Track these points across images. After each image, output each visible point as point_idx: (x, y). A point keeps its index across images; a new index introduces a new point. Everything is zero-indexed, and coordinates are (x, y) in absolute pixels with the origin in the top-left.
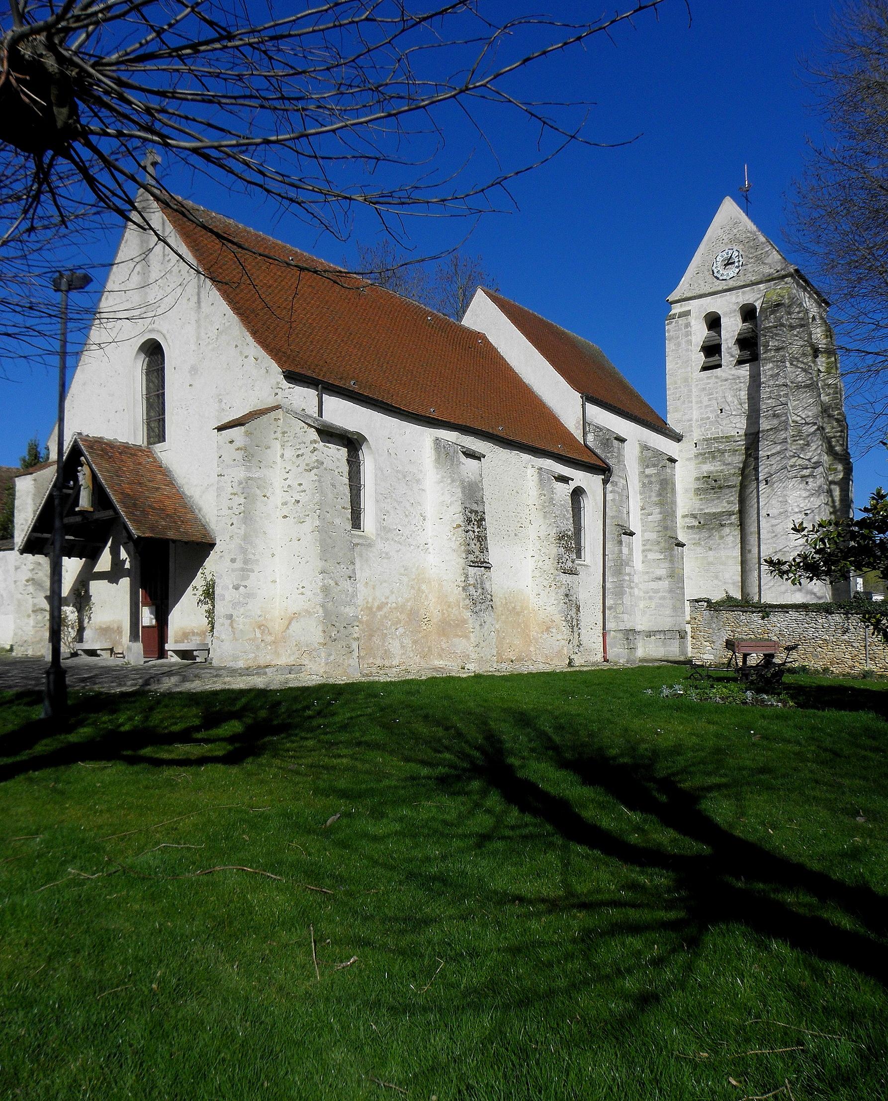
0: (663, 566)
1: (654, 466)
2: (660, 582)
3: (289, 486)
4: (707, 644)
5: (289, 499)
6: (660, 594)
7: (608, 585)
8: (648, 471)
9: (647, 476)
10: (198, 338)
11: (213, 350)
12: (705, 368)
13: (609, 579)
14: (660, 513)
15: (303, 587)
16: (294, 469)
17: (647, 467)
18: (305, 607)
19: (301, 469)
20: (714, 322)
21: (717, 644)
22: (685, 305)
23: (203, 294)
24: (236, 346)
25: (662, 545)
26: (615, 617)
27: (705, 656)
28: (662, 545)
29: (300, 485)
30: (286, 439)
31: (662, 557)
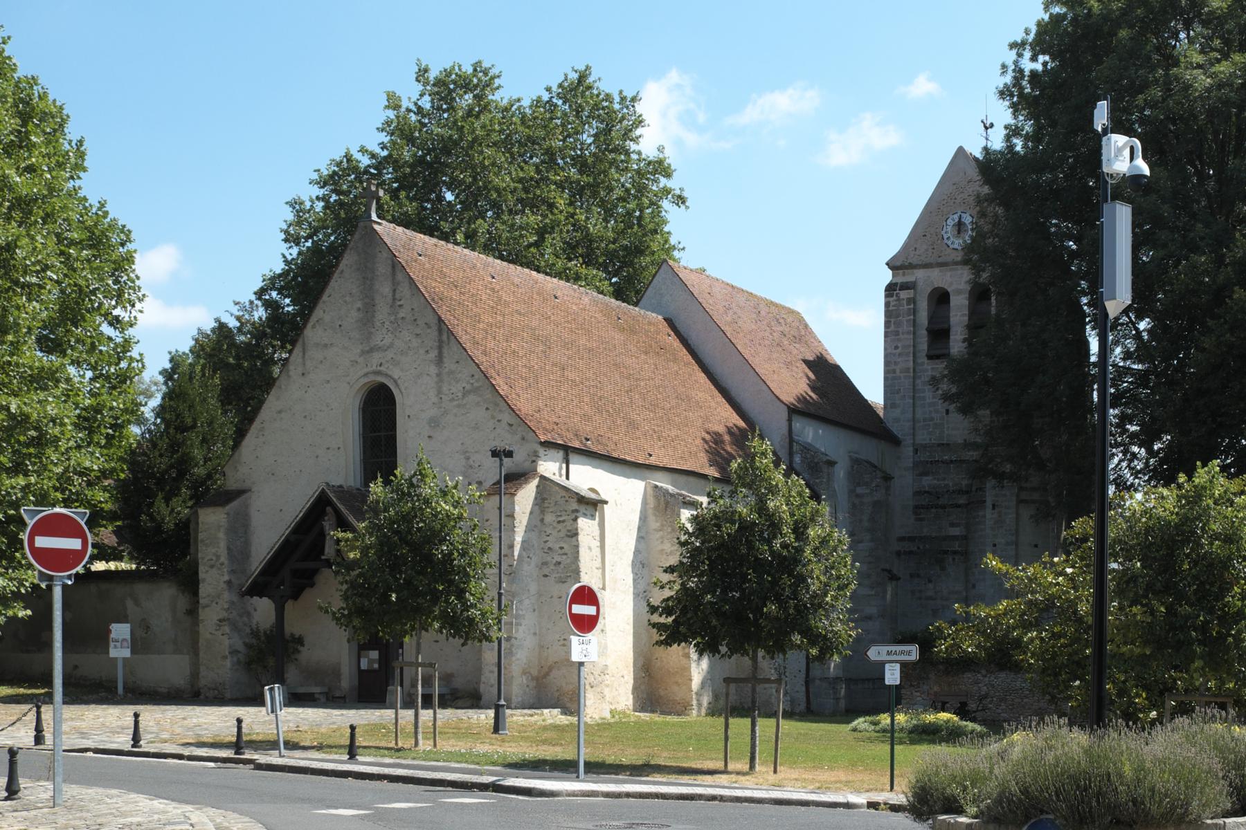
5: (549, 559)
8: (859, 490)
9: (858, 496)
10: (439, 392)
11: (458, 406)
16: (554, 533)
17: (858, 484)
19: (562, 534)
23: (445, 351)
29: (562, 548)
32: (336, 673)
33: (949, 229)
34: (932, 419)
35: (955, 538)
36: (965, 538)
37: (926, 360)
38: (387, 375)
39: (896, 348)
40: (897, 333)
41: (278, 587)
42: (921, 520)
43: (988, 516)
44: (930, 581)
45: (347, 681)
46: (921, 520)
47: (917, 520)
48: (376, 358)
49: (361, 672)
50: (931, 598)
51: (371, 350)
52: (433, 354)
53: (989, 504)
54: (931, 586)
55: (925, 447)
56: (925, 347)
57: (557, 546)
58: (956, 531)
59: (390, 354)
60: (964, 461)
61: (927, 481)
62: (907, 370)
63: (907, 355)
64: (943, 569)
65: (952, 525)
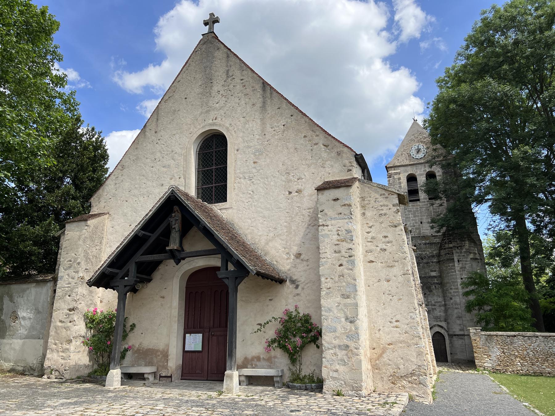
3: (373, 238)
4: (486, 356)
15: (397, 321)
18: (401, 338)
20: (412, 179)
22: (396, 170)
24: (305, 137)
27: (485, 364)
29: (385, 237)
30: (366, 202)
32: (165, 355)
33: (413, 152)
38: (220, 125)
41: (123, 278)
43: (456, 265)
45: (174, 361)
48: (212, 114)
49: (185, 352)
51: (208, 112)
52: (259, 105)
53: (456, 260)
57: (380, 236)
58: (433, 274)
59: (222, 112)
64: (431, 291)
65: (432, 271)
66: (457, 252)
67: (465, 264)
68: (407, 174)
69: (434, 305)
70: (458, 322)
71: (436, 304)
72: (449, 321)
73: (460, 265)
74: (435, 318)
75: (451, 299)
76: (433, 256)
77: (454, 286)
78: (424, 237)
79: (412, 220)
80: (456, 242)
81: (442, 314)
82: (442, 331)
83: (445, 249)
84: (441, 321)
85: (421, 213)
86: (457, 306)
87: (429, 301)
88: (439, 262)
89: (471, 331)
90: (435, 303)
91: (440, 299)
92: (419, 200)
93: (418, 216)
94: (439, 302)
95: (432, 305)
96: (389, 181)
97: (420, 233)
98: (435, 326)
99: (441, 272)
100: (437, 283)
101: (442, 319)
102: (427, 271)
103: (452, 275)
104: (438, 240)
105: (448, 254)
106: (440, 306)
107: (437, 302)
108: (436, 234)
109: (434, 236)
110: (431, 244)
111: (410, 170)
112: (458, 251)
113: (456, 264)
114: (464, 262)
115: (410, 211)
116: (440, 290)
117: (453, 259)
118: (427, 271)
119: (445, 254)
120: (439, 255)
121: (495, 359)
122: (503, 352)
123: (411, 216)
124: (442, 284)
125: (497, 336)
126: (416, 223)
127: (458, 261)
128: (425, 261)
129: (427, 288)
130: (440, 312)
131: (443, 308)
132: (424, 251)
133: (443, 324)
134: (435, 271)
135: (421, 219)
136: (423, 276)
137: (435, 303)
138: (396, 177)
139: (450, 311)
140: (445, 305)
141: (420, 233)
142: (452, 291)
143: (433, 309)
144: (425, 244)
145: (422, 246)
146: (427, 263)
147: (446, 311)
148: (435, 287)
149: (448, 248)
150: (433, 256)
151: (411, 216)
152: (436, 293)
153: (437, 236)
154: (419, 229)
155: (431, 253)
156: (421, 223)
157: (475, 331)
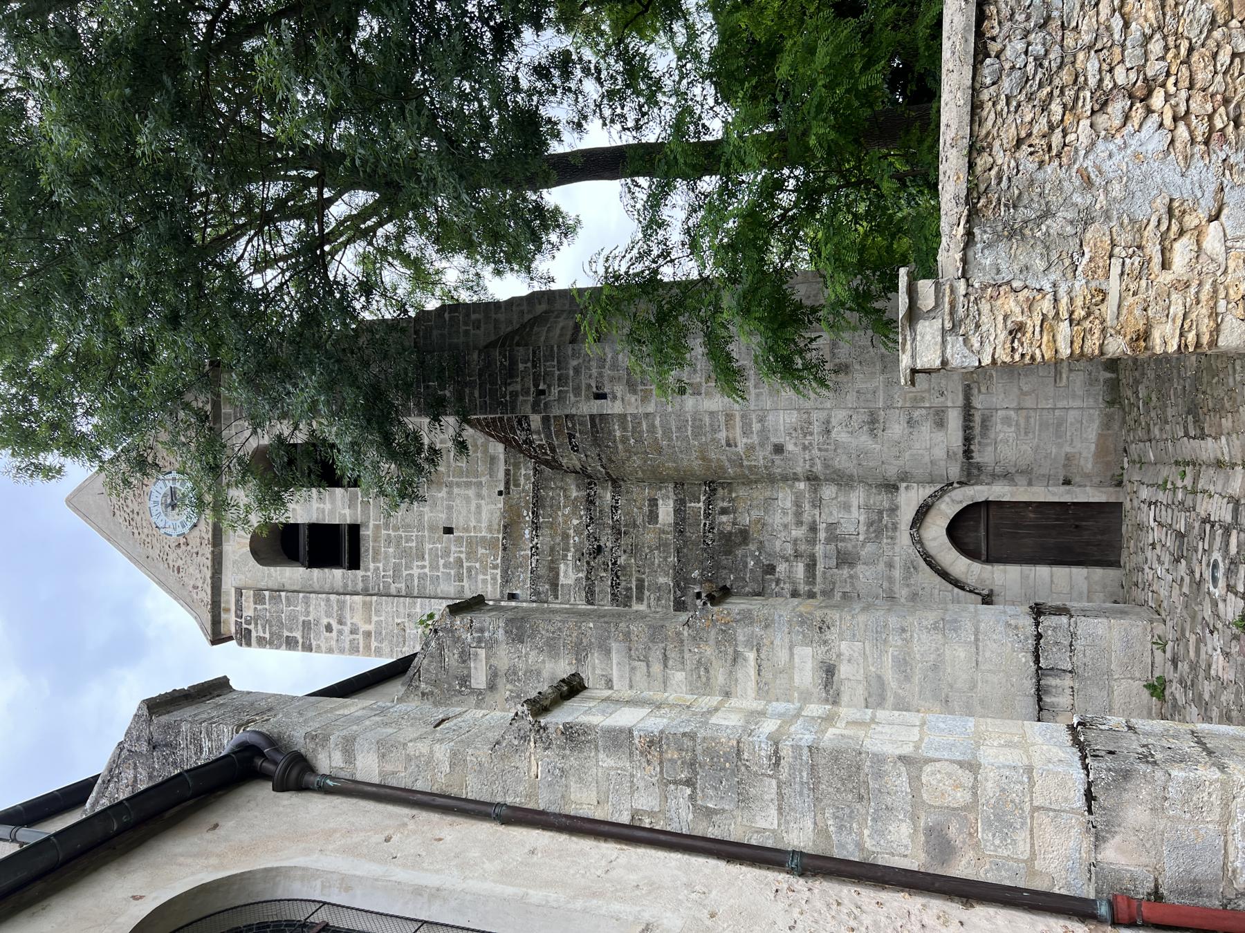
0: (782, 655)
1: (465, 657)
2: (844, 670)
4: (1181, 252)
6: (890, 676)
7: (800, 837)
8: (479, 679)
9: (492, 687)
12: (355, 564)
13: (761, 824)
14: (608, 652)
17: (465, 680)
21: (1182, 188)
22: (228, 602)
25: (709, 651)
26: (1002, 823)
28: (709, 651)
31: (751, 656)
34: (459, 562)
35: (679, 511)
36: (679, 484)
37: (360, 573)
39: (329, 628)
40: (306, 625)
42: (640, 588)
44: (771, 569)
46: (640, 588)
47: (640, 599)
50: (811, 567)
53: (595, 407)
54: (782, 568)
55: (506, 581)
56: (338, 573)
58: (666, 512)
60: (536, 496)
61: (569, 575)
62: (367, 606)
63: (341, 606)
64: (744, 535)
65: (653, 517)
66: (562, 398)
67: (614, 366)
68: (252, 561)
69: (813, 529)
70: (897, 429)
71: (806, 518)
72: (892, 472)
73: (619, 389)
74: (879, 533)
75: (779, 449)
76: (590, 501)
77: (715, 430)
78: (510, 528)
79: (434, 567)
80: (514, 395)
81: (857, 497)
82: (947, 509)
83: (553, 450)
84: (894, 510)
85: (407, 527)
86: (816, 428)
87: (789, 550)
88: (615, 483)
89: (929, 358)
90: (799, 523)
91: (785, 498)
92: (355, 529)
93: (421, 541)
94: (798, 505)
95: (812, 541)
96: (262, 642)
97: (491, 544)
98: (918, 541)
99: (657, 479)
100: (709, 502)
101: (883, 500)
102: (649, 537)
103: (667, 432)
104: (526, 471)
105: (571, 436)
106: (817, 503)
107: (798, 514)
108: (501, 475)
109: (507, 483)
110: (538, 503)
111: (237, 545)
112: (555, 391)
113: (612, 408)
114: (607, 372)
115: (397, 569)
116: (742, 492)
117: (592, 417)
118: (649, 537)
119: (575, 449)
120: (586, 478)
121: (1205, 172)
122: (1141, 95)
123: (416, 572)
124: (713, 484)
125: (975, 149)
126: (447, 553)
127: (601, 396)
128: (607, 541)
129: (729, 553)
130: (847, 507)
131: (828, 491)
132: (566, 537)
133: (909, 500)
134: (653, 503)
135: (432, 529)
136: (672, 559)
137: (799, 523)
138: (248, 612)
139: (842, 462)
140: (812, 478)
141: (491, 544)
142: (742, 442)
143: (833, 538)
144: (536, 527)
145: (544, 541)
146: (618, 533)
147: (844, 481)
148: (724, 511)
149: (549, 436)
150: (590, 501)
151: (416, 572)
152: (755, 514)
153: (507, 472)
154: (471, 543)
155: (575, 508)
156: (448, 531)
157: (928, 331)
